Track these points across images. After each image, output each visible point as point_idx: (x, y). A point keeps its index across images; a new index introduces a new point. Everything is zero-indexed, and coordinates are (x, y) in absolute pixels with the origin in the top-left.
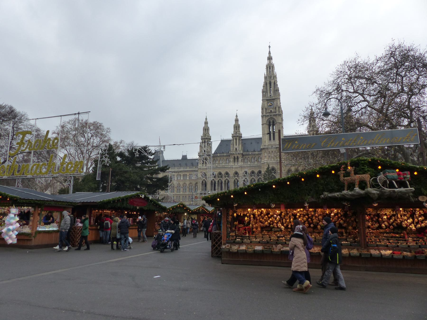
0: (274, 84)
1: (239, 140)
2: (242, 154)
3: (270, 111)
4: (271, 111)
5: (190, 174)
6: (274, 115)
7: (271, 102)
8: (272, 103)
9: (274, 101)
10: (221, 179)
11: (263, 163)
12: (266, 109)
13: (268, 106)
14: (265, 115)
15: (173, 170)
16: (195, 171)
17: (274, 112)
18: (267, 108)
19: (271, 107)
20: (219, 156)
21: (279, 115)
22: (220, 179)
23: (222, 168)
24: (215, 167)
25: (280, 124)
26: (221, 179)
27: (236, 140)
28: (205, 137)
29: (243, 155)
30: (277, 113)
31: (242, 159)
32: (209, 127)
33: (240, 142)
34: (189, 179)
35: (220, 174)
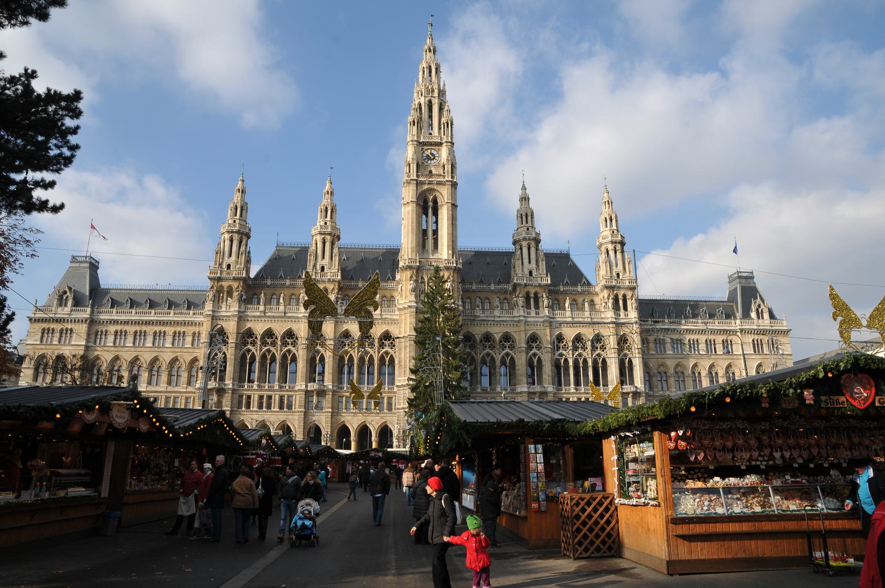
0: (441, 109)
1: (333, 244)
2: (339, 282)
3: (428, 173)
4: (431, 172)
5: (175, 333)
6: (439, 183)
7: (433, 151)
8: (435, 153)
9: (439, 149)
10: (272, 349)
11: (405, 308)
12: (418, 165)
13: (424, 160)
14: (416, 180)
15: (123, 318)
16: (192, 324)
17: (439, 175)
18: (420, 163)
19: (432, 162)
20: (268, 287)
21: (452, 185)
22: (269, 351)
23: (278, 317)
24: (258, 314)
25: (454, 207)
26: (272, 349)
27: (324, 243)
28: (235, 226)
29: (340, 289)
30: (446, 179)
31: (339, 296)
32: (246, 204)
33: (336, 251)
34: (171, 346)
35: (269, 333)
